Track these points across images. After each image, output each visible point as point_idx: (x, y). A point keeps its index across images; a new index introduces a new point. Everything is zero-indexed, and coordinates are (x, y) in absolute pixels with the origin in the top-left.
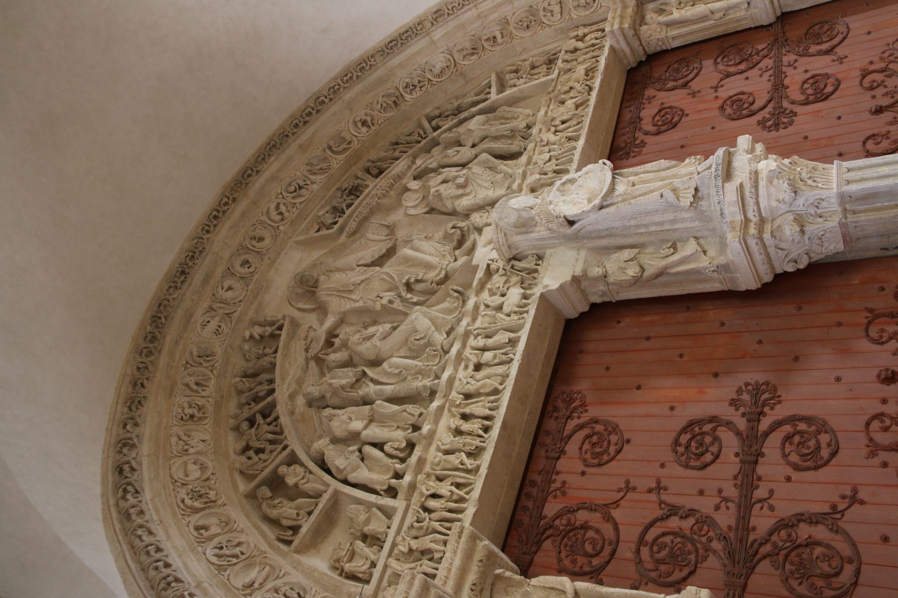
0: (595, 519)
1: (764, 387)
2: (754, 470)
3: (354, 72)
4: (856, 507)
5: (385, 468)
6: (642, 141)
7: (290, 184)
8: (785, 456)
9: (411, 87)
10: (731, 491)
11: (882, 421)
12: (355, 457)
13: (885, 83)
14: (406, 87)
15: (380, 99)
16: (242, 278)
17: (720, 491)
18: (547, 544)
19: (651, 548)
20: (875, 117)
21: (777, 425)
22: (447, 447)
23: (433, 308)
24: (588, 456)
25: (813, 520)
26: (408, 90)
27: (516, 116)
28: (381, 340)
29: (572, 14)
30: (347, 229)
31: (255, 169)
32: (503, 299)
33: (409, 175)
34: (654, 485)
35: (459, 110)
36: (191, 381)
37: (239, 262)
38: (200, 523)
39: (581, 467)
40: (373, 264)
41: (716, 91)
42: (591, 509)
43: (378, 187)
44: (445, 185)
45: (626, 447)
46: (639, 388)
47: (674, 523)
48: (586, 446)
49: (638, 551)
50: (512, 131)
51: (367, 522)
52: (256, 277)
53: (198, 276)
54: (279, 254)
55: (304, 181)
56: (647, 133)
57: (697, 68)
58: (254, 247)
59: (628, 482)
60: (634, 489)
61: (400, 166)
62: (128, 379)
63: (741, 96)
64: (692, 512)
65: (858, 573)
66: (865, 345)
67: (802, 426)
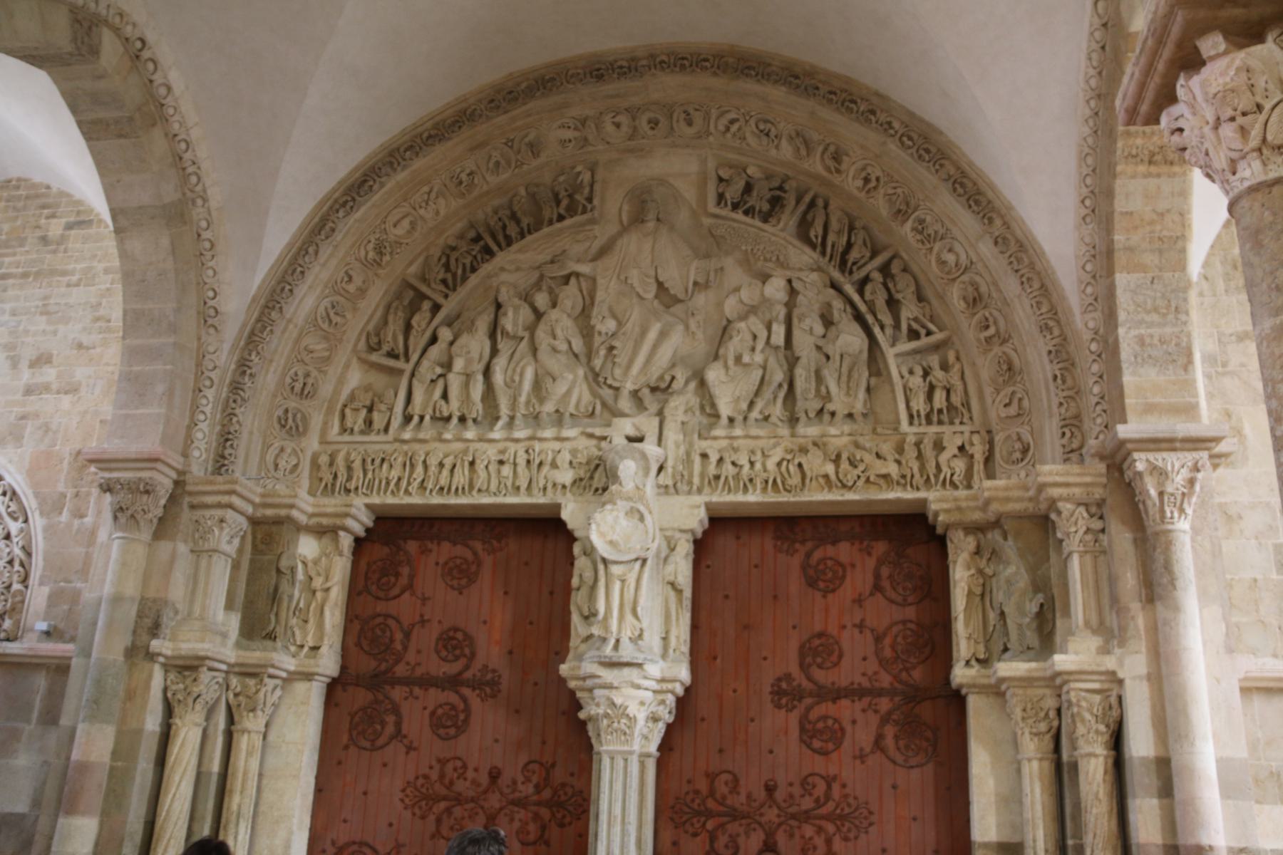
0: (404, 581)
1: (496, 688)
2: (432, 686)
3: (916, 148)
4: (404, 750)
5: (425, 407)
6: (797, 551)
7: (766, 121)
8: (440, 706)
9: (920, 227)
10: (419, 671)
11: (461, 768)
12: (429, 377)
13: (807, 798)
14: (924, 221)
15: (899, 191)
16: (635, 129)
17: (419, 664)
18: (386, 550)
19: (380, 624)
20: (763, 783)
21: (464, 700)
22: (428, 462)
23: (585, 387)
24: (451, 564)
25: (398, 724)
26: (916, 225)
27: (851, 392)
28: (549, 345)
29: (1001, 434)
30: (720, 222)
31: (759, 77)
32: (567, 465)
33: (789, 274)
34: (426, 618)
35: (892, 304)
36: (496, 155)
37: (652, 115)
38: (351, 272)
39: (441, 561)
40: (660, 285)
41: (855, 626)
42: (412, 577)
43: (773, 238)
44: (749, 337)
45: (456, 592)
46: (506, 593)
47: (399, 636)
48: (458, 561)
49: (379, 615)
50: (828, 392)
51: (380, 411)
52: (644, 141)
53: (609, 88)
54: (688, 146)
55: (776, 137)
56: (808, 555)
57: (905, 600)
58: (678, 121)
59: (429, 599)
60: (424, 604)
61: (802, 256)
62: (464, 105)
63: (836, 653)
64: (405, 648)
65: (365, 749)
66: (523, 759)
67: (462, 717)
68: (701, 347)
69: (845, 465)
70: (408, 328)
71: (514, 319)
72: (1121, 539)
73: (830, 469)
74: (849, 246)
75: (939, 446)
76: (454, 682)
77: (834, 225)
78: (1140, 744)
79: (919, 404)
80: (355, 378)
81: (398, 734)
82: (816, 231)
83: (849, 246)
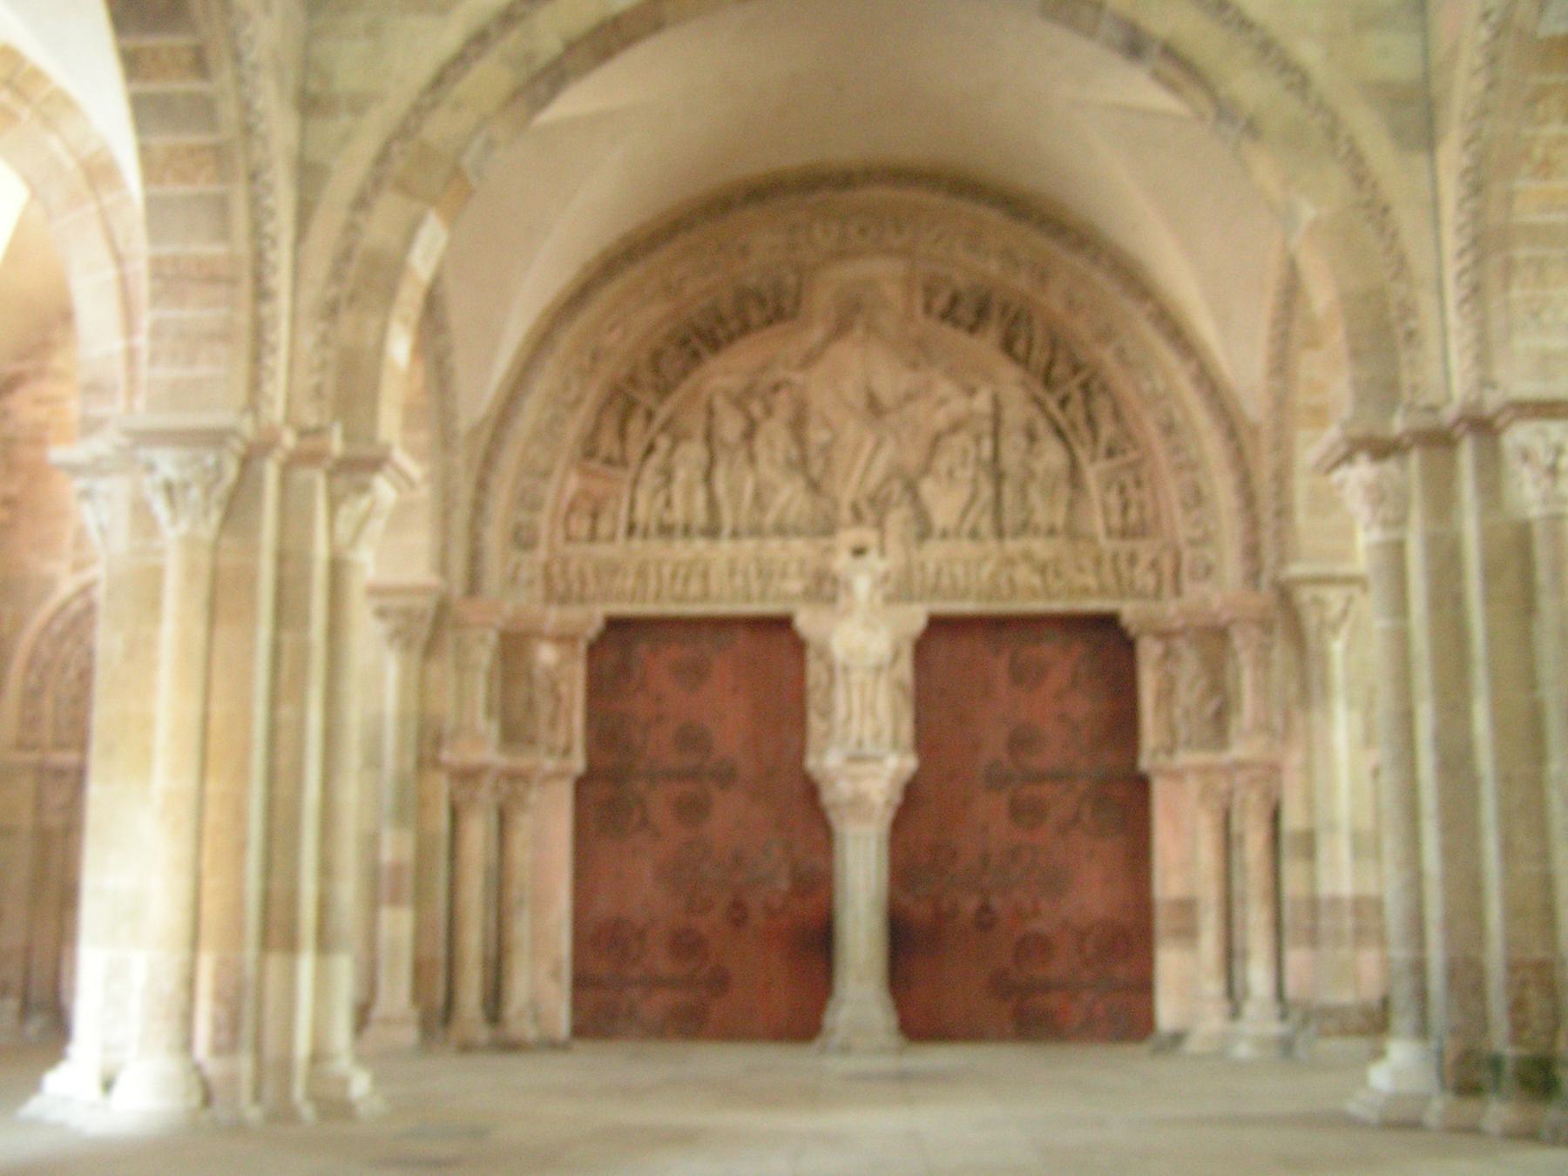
61: (1009, 374)
68: (913, 457)
69: (1050, 577)
70: (622, 435)
71: (730, 427)
72: (1280, 653)
73: (1036, 580)
74: (1050, 365)
75: (1133, 560)
76: (693, 775)
77: (1039, 339)
78: (1293, 820)
79: (1116, 520)
80: (573, 483)
81: (645, 822)
82: (1020, 347)
83: (1050, 365)
